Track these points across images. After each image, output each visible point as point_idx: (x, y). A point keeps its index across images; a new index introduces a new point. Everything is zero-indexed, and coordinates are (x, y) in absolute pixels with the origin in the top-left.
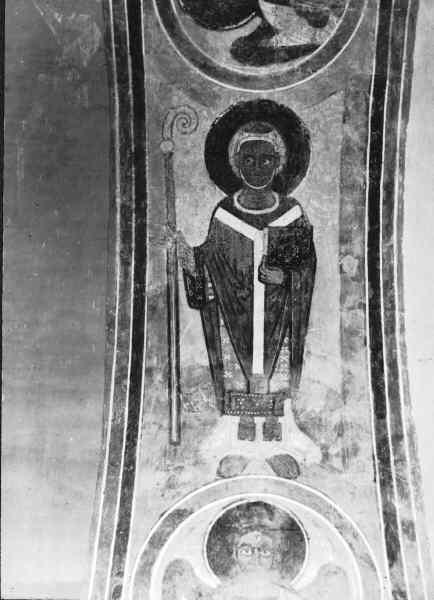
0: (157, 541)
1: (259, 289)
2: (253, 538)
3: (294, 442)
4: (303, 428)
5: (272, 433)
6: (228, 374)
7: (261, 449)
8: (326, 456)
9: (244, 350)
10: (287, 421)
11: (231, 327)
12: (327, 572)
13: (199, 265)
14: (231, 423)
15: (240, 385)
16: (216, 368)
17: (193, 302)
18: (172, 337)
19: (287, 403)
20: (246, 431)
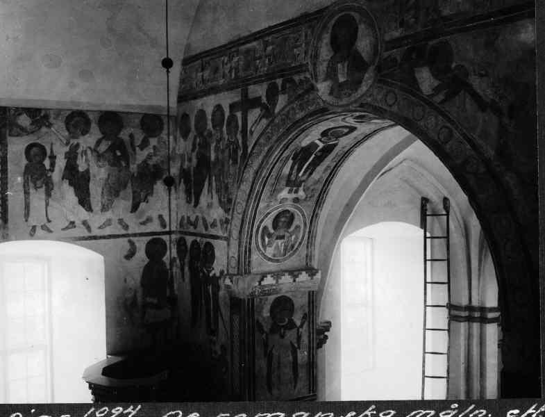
0: (261, 222)
1: (313, 156)
2: (283, 219)
3: (301, 193)
4: (304, 190)
5: (296, 192)
6: (292, 176)
7: (294, 196)
8: (306, 198)
9: (299, 170)
10: (301, 188)
11: (299, 165)
12: (298, 227)
13: (300, 152)
14: (288, 188)
15: (294, 179)
16: (290, 174)
17: (293, 159)
18: (284, 165)
19: (303, 184)
20: (290, 192)
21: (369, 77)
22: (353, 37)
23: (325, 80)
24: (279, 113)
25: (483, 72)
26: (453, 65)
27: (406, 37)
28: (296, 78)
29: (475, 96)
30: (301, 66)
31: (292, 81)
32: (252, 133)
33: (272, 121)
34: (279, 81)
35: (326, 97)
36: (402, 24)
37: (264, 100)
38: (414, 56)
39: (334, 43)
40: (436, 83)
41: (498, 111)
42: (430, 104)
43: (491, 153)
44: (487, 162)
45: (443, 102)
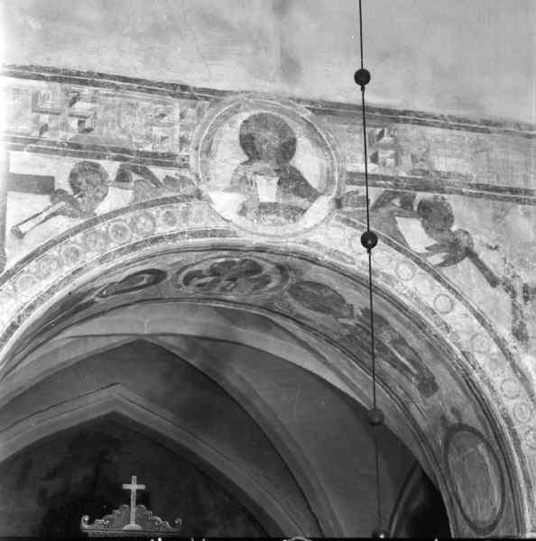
21: (323, 205)
22: (288, 149)
23: (231, 190)
24: (108, 216)
25: (494, 246)
26: (454, 228)
27: (385, 178)
28: (159, 173)
29: (482, 267)
30: (171, 156)
31: (145, 173)
32: (20, 235)
33: (89, 224)
34: (111, 167)
35: (232, 215)
36: (375, 159)
37: (63, 183)
38: (397, 202)
39: (248, 144)
40: (432, 242)
41: (509, 289)
42: (423, 265)
43: (505, 332)
44: (500, 342)
45: (442, 265)
